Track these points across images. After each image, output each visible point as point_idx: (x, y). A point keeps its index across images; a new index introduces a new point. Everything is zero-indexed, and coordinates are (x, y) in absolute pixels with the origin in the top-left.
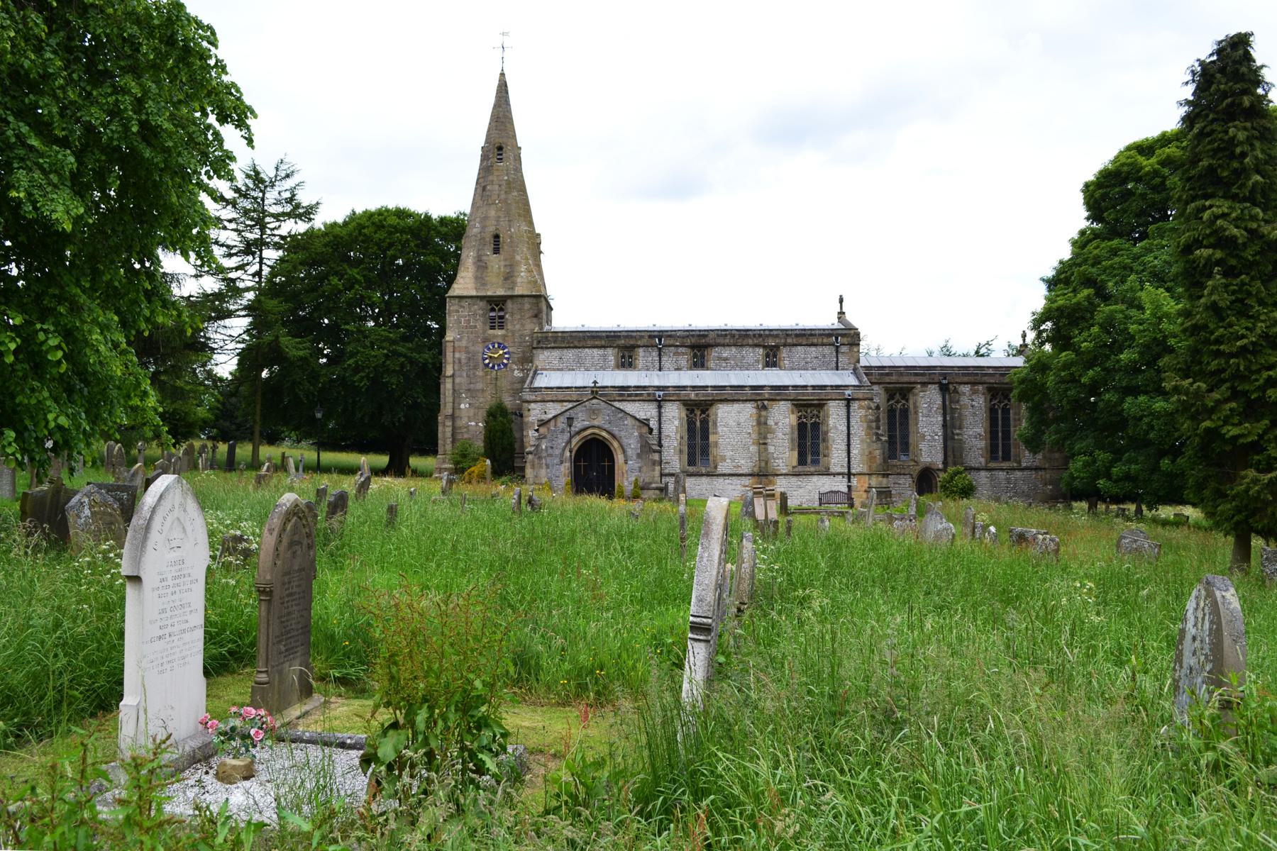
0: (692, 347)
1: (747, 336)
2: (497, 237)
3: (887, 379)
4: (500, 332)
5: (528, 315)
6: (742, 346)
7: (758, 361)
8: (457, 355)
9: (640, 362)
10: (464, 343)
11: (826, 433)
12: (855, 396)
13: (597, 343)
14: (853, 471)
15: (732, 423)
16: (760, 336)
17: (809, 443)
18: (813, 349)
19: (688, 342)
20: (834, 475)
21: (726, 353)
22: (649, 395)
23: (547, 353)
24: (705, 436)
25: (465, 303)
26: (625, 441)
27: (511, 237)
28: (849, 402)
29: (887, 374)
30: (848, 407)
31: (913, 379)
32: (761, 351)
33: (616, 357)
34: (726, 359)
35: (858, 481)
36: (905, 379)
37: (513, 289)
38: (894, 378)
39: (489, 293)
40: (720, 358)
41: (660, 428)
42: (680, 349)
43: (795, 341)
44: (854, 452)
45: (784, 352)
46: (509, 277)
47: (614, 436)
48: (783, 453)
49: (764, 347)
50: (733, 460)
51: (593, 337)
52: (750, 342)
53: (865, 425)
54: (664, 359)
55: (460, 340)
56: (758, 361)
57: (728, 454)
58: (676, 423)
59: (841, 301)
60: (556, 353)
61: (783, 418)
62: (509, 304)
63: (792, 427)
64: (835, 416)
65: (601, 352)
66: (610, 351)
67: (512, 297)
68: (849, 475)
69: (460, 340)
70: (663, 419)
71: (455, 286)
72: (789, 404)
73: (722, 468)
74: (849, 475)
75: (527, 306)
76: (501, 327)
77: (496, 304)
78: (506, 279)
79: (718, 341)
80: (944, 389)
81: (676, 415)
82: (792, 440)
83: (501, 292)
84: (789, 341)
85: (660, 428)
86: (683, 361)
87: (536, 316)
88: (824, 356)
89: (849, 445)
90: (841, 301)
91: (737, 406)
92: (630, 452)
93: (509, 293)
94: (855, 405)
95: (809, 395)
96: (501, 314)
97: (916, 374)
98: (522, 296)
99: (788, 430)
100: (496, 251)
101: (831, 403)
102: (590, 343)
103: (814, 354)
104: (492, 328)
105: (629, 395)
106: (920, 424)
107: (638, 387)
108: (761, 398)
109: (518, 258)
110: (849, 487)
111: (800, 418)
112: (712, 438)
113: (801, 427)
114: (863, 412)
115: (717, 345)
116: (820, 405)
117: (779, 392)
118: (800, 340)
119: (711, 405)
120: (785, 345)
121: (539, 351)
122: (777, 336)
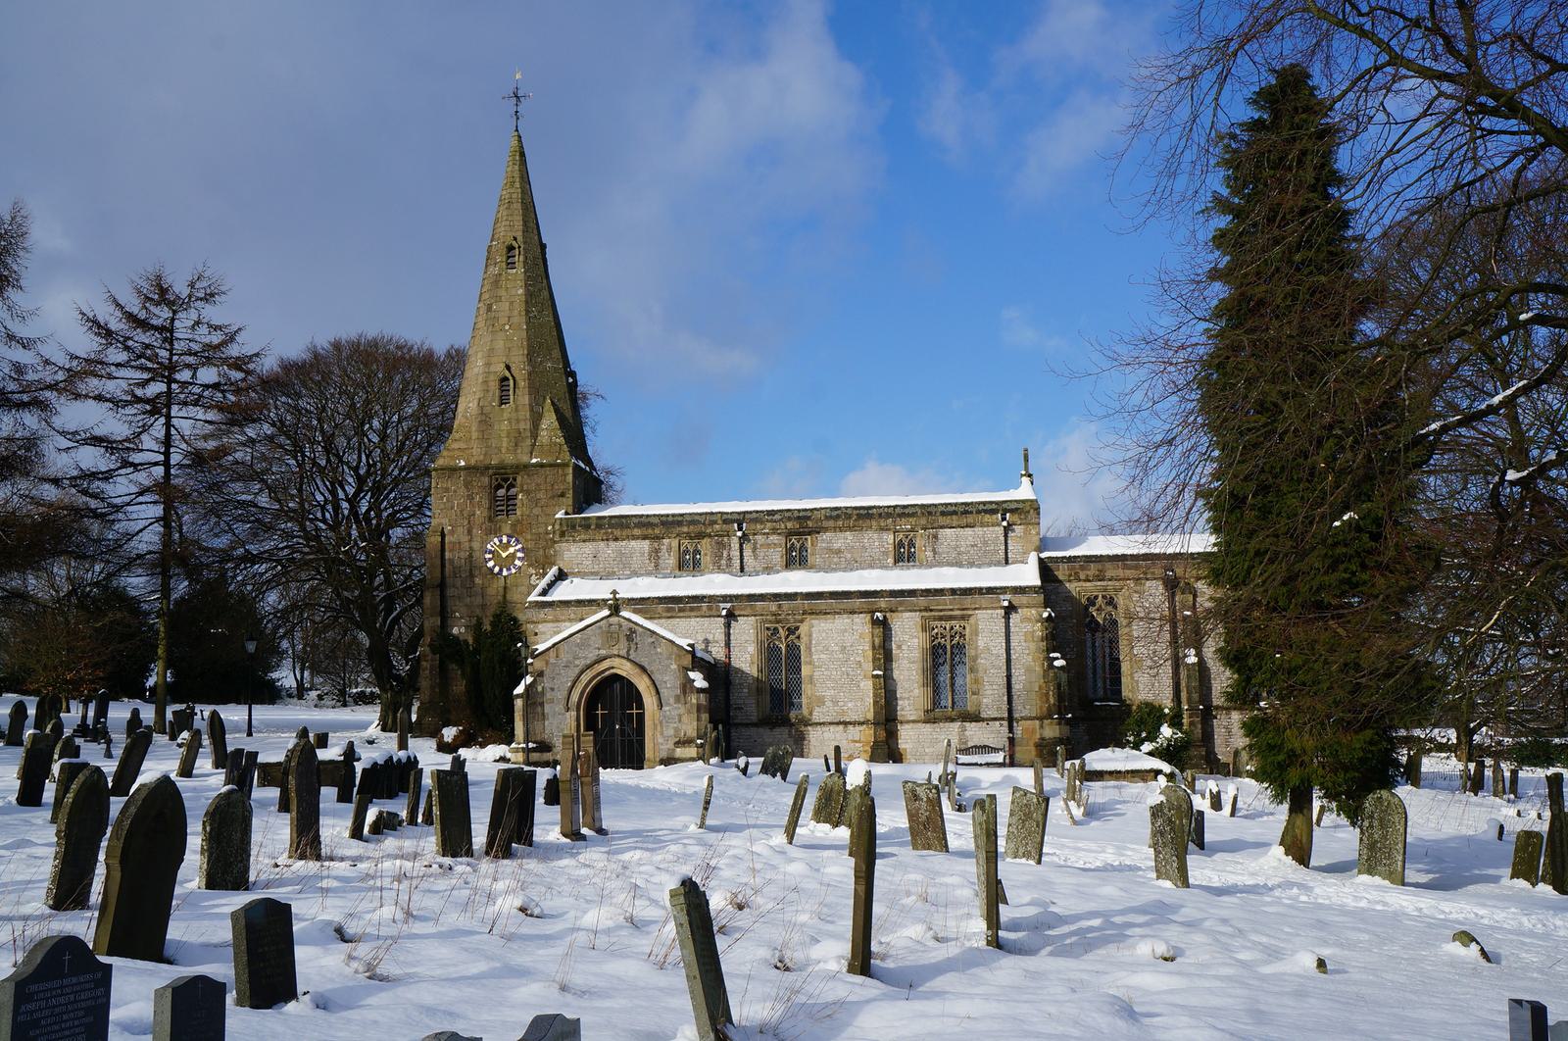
7: (886, 553)
11: (975, 659)
14: (1016, 715)
21: (842, 540)
26: (657, 677)
30: (1007, 617)
34: (839, 552)
40: (830, 550)
47: (643, 669)
50: (835, 703)
57: (829, 693)
58: (752, 649)
60: (589, 548)
61: (909, 637)
64: (986, 632)
80: (1172, 585)
81: (753, 638)
86: (777, 556)
88: (985, 543)
91: (842, 622)
92: (664, 692)
94: (1014, 618)
99: (917, 655)
102: (637, 532)
112: (805, 671)
114: (1029, 627)
115: (826, 530)
118: (947, 520)
119: (802, 621)
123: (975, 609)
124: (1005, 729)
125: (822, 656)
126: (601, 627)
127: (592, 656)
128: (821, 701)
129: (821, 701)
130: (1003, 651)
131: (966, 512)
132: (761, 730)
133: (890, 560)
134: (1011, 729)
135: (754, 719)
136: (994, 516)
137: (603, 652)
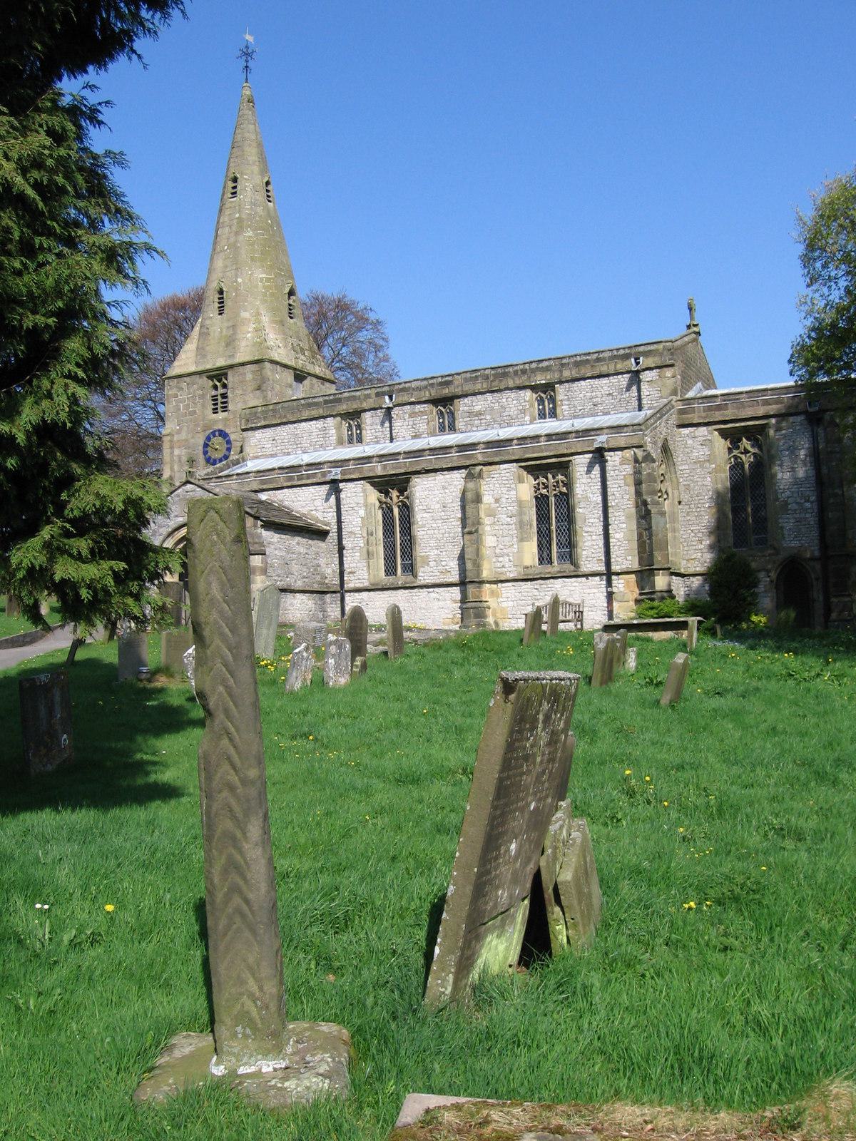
0: (434, 402)
1: (505, 375)
2: (221, 292)
3: (718, 416)
4: (221, 415)
5: (250, 389)
6: (499, 391)
7: (523, 412)
8: (177, 452)
9: (368, 433)
10: (183, 436)
12: (613, 444)
13: (314, 413)
14: (615, 568)
17: (554, 525)
18: (605, 381)
19: (426, 395)
20: (586, 576)
21: (479, 403)
23: (258, 434)
27: (236, 289)
29: (719, 408)
32: (528, 394)
33: (338, 428)
34: (479, 414)
36: (749, 413)
37: (233, 356)
38: (729, 414)
39: (209, 366)
40: (470, 414)
41: (339, 522)
42: (418, 408)
43: (575, 374)
44: (617, 536)
46: (230, 342)
49: (534, 388)
50: (438, 561)
51: (309, 405)
52: (511, 383)
54: (396, 423)
55: (179, 432)
56: (523, 412)
58: (362, 512)
61: (509, 492)
62: (230, 373)
63: (520, 503)
67: (232, 367)
68: (609, 575)
69: (179, 432)
70: (343, 508)
71: (176, 363)
73: (425, 575)
74: (609, 575)
75: (249, 376)
76: (225, 409)
77: (218, 376)
78: (228, 345)
79: (468, 388)
82: (521, 525)
83: (221, 362)
84: (567, 374)
85: (339, 522)
86: (423, 427)
87: (259, 388)
91: (440, 478)
93: (230, 362)
94: (613, 459)
95: (544, 450)
96: (224, 391)
98: (243, 364)
100: (221, 311)
103: (606, 390)
104: (215, 411)
105: (300, 478)
107: (310, 465)
108: (471, 463)
109: (245, 315)
110: (610, 596)
111: (537, 489)
115: (466, 396)
116: (563, 467)
117: (498, 451)
120: (561, 382)
121: (250, 433)
122: (548, 369)
123: (573, 454)
126: (178, 496)
129: (426, 561)
130: (600, 499)
131: (598, 360)
133: (527, 418)
134: (609, 584)
135: (366, 584)
136: (627, 363)
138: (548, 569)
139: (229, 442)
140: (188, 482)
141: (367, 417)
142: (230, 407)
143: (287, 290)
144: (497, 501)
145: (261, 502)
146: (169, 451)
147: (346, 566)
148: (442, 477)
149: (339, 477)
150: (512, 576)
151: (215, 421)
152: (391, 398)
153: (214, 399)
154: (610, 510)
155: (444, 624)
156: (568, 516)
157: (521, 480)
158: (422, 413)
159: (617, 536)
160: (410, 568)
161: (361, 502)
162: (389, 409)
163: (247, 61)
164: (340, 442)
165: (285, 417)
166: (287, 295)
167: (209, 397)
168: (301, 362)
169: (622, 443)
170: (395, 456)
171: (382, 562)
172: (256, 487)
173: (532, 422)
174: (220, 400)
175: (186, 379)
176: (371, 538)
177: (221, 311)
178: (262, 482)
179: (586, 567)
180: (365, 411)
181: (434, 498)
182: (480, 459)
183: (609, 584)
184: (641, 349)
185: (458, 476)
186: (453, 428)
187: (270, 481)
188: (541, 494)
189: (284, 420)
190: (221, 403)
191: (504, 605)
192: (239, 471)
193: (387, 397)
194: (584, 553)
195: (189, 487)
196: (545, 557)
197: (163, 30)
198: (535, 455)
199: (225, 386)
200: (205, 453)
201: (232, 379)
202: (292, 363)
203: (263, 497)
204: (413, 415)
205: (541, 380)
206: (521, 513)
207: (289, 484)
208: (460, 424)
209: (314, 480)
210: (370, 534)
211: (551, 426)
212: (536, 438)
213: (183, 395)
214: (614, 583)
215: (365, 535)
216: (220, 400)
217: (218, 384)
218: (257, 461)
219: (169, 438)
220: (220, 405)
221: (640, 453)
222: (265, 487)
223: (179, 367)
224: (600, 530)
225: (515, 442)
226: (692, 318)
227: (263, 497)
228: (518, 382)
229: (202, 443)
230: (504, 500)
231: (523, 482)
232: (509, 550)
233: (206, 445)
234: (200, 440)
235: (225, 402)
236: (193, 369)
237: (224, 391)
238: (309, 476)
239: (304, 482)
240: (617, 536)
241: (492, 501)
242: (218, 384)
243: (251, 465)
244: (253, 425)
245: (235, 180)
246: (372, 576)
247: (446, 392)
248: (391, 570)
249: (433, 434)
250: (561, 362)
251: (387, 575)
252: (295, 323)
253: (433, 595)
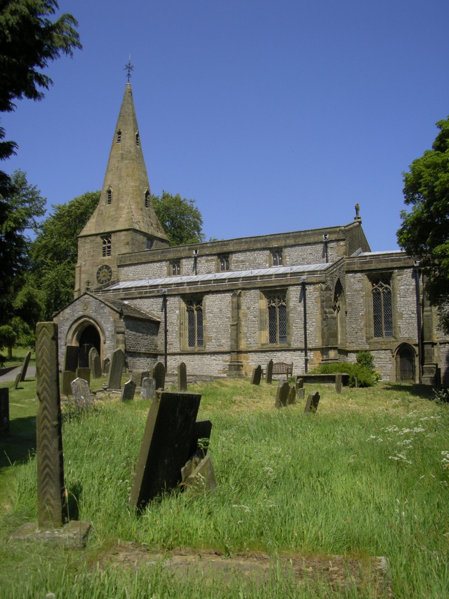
2: (109, 192)
4: (107, 257)
8: (83, 276)
12: (309, 281)
14: (309, 346)
15: (216, 310)
16: (266, 240)
17: (277, 322)
20: (295, 350)
22: (158, 291)
24: (200, 323)
25: (88, 240)
28: (304, 285)
29: (367, 262)
31: (390, 265)
32: (267, 252)
33: (168, 267)
35: (315, 355)
36: (383, 265)
37: (115, 226)
38: (373, 266)
39: (102, 231)
40: (237, 262)
41: (166, 317)
42: (209, 258)
44: (310, 329)
45: (286, 252)
48: (256, 335)
49: (270, 249)
53: (319, 305)
54: (199, 265)
57: (213, 335)
58: (177, 312)
59: (357, 209)
61: (255, 304)
65: (158, 264)
66: (164, 263)
69: (85, 265)
72: (258, 291)
73: (210, 346)
75: (123, 237)
76: (109, 254)
77: (106, 236)
82: (261, 322)
83: (108, 230)
85: (166, 317)
89: (305, 323)
90: (357, 209)
92: (107, 334)
93: (113, 230)
94: (310, 289)
95: (274, 282)
96: (109, 245)
97: (393, 261)
100: (109, 202)
101: (291, 288)
103: (309, 251)
104: (104, 255)
105: (146, 293)
106: (398, 304)
108: (235, 289)
110: (306, 361)
113: (271, 309)
115: (235, 252)
124: (303, 354)
125: (210, 315)
127: (77, 316)
128: (210, 339)
129: (210, 339)
130: (303, 309)
131: (305, 235)
132: (181, 356)
133: (267, 265)
134: (306, 355)
135: (178, 351)
137: (81, 313)
138: (274, 345)
139: (111, 272)
140: (86, 294)
141: (184, 262)
142: (112, 253)
143: (145, 192)
144: (249, 308)
145: (125, 305)
146: (79, 275)
147: (168, 340)
148: (220, 295)
149: (166, 293)
150: (254, 349)
151: (104, 261)
152: (196, 252)
153: (104, 249)
154: (307, 315)
155: (219, 373)
156: (284, 319)
157: (261, 298)
158: (212, 260)
159: (311, 329)
160: (201, 343)
161: (177, 306)
162: (196, 259)
163: (129, 71)
164: (169, 274)
165: (140, 260)
166: (144, 195)
167: (101, 247)
168: (151, 231)
169: (314, 280)
170: (196, 283)
171: (187, 339)
172: (122, 296)
173: (270, 267)
174: (107, 249)
175: (89, 238)
176: (182, 326)
177: (109, 202)
178: (126, 294)
179: (295, 345)
180: (182, 258)
181: (216, 306)
182: (240, 286)
183: (306, 355)
184: (328, 230)
185: (228, 294)
186: (228, 269)
187: (131, 294)
188: (272, 306)
189: (140, 262)
190: (107, 251)
191: (250, 364)
192: (114, 288)
193: (194, 251)
194: (293, 337)
195: (86, 296)
196: (272, 339)
197: (58, 59)
198: (269, 285)
199: (109, 242)
200: (98, 277)
201: (113, 238)
202: (146, 231)
203: (126, 302)
204: (207, 261)
205: (275, 245)
206: (261, 316)
207: (140, 296)
208: (232, 266)
209: (153, 294)
210: (181, 324)
211: (226, 275)
212: (270, 276)
213: (88, 246)
214: (308, 354)
215: (179, 324)
216: (107, 249)
217: (106, 241)
218: (124, 283)
219: (79, 268)
220: (106, 253)
221: (324, 286)
222: (127, 297)
223: (85, 231)
224: (302, 326)
225: (259, 278)
226: (357, 213)
227: (126, 302)
228: (263, 245)
229: (96, 271)
230: (252, 308)
231: (263, 299)
232: (254, 335)
233: (98, 273)
234: (96, 270)
235: (110, 251)
236: (93, 232)
237: (109, 245)
238: (150, 292)
239: (148, 295)
240: (311, 329)
241: (246, 308)
242: (106, 241)
243: (123, 285)
244: (124, 264)
245: (120, 133)
246: (181, 347)
247: (225, 249)
248: (191, 344)
249: (218, 271)
250: (287, 236)
251: (190, 346)
252: (149, 210)
253: (213, 357)
